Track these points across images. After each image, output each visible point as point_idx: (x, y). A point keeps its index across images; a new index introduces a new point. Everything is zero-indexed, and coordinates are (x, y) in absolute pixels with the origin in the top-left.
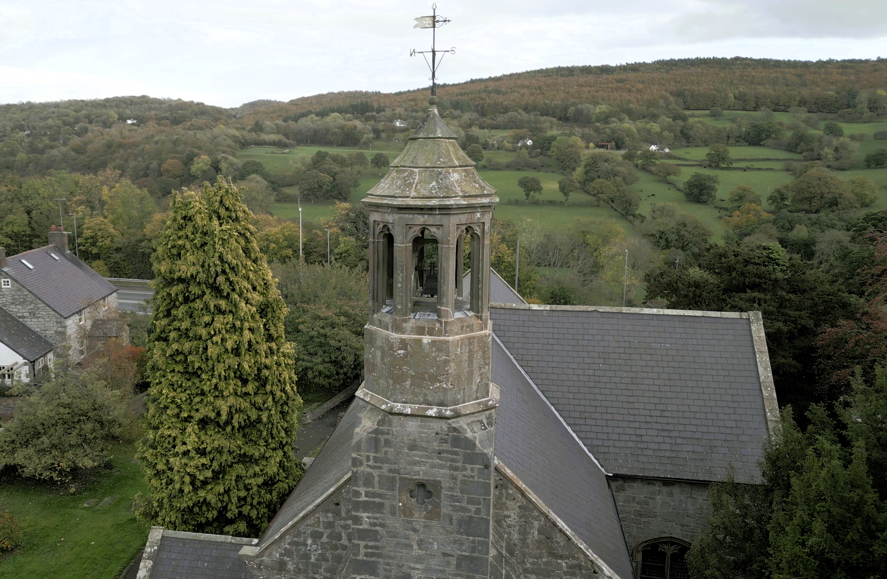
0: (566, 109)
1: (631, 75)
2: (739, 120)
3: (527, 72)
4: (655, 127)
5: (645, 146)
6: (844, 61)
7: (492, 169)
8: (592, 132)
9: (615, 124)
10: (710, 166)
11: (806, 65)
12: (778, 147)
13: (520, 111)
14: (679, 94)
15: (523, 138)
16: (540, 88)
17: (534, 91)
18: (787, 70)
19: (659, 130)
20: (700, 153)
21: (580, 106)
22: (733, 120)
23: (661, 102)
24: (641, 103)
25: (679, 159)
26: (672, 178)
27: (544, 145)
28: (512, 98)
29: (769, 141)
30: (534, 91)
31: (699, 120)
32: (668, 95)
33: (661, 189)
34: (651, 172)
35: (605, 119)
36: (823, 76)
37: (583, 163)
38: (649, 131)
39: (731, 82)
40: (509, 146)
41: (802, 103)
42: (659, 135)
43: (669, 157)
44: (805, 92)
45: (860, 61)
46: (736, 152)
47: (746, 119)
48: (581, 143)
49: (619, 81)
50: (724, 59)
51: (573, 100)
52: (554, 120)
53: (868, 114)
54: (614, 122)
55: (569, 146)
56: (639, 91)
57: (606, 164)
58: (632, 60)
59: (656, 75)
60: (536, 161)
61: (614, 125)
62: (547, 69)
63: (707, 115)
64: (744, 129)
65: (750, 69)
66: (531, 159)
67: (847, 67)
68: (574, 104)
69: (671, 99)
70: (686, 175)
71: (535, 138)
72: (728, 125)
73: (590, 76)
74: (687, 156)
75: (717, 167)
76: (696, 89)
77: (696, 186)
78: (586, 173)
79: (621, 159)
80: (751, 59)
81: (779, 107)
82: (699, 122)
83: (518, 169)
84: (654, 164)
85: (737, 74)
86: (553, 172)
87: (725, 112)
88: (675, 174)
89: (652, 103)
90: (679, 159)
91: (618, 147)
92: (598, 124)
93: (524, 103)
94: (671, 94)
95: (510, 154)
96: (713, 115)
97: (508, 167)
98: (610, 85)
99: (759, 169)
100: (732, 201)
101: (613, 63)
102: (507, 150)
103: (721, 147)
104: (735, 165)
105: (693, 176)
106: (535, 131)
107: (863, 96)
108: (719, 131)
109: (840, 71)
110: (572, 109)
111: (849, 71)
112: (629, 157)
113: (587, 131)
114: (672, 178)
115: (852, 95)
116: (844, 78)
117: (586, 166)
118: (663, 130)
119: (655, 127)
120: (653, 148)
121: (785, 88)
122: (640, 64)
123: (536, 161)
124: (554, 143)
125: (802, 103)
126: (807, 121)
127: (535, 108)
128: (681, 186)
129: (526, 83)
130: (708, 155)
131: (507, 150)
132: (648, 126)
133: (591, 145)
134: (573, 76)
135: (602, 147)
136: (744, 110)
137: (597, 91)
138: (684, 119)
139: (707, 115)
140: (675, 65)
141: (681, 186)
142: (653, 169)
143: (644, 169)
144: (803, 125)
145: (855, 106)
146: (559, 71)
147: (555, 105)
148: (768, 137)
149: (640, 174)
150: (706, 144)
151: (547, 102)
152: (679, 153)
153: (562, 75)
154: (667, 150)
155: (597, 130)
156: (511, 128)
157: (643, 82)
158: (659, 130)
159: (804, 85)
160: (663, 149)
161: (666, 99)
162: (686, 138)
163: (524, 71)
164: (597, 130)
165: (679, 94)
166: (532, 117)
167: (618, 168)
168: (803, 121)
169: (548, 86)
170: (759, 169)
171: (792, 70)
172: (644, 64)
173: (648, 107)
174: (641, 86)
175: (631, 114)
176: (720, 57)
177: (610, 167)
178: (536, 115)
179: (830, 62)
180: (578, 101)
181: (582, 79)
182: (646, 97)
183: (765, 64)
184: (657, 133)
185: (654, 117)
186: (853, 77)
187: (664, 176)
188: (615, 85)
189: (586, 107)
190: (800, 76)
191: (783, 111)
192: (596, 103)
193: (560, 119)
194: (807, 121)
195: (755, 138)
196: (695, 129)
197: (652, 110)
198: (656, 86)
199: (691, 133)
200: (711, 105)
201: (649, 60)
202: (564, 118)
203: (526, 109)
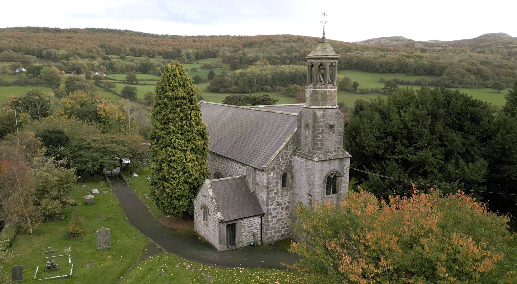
0: (41, 51)
1: (74, 34)
2: (135, 60)
3: (8, 28)
4: (96, 63)
5: (93, 73)
6: (173, 36)
7: (3, 85)
8: (62, 65)
9: (73, 61)
10: (128, 83)
11: (157, 36)
12: (155, 74)
13: (11, 51)
14: (103, 46)
15: (18, 67)
16: (20, 38)
17: (16, 40)
18: (150, 38)
19: (98, 64)
20: (123, 77)
21: (49, 50)
22: (132, 61)
23: (94, 50)
24: (84, 50)
25: (112, 79)
26: (112, 89)
27: (35, 72)
28: (3, 43)
29: (151, 72)
30: (16, 40)
31: (115, 59)
32: (97, 47)
33: (108, 95)
34: (101, 86)
35: (67, 58)
36: (166, 42)
37: (65, 82)
38: (93, 65)
39: (127, 42)
40: (11, 71)
41: (160, 54)
42: (99, 67)
43: (106, 78)
44: (160, 49)
45: (179, 36)
46: (139, 76)
47: (138, 61)
48: (58, 71)
49: (68, 37)
50: (120, 30)
51: (44, 46)
52: (35, 57)
53: (186, 60)
54: (72, 60)
55: (52, 72)
56: (81, 44)
57: (78, 82)
58: (73, 27)
59: (88, 36)
60: (33, 80)
61: (73, 61)
62: (21, 28)
63: (118, 58)
64: (138, 65)
65: (133, 36)
66: (29, 80)
67: (174, 39)
68: (44, 49)
69: (99, 49)
70: (120, 88)
71: (27, 67)
72: (131, 63)
73: (50, 33)
74: (115, 78)
75: (132, 84)
76: (110, 44)
77: (126, 93)
78: (67, 87)
79: (85, 79)
80: (133, 31)
81: (151, 55)
82: (118, 61)
83: (22, 85)
84: (102, 82)
85: (128, 38)
86: (45, 87)
87: (127, 57)
88: (114, 87)
89: (90, 51)
90: (112, 79)
91: (78, 72)
92: (63, 60)
93: (12, 46)
94: (98, 46)
95: (13, 76)
96: (122, 58)
97: (15, 84)
98: (63, 39)
99: (150, 84)
100: (145, 99)
101: (62, 27)
102: (10, 74)
103: (132, 73)
104: (140, 82)
105: (124, 88)
106: (25, 64)
107: (184, 52)
108: (127, 66)
109: (172, 40)
110: (44, 52)
111: (175, 40)
112: (88, 78)
113: (58, 64)
114: (112, 89)
115: (179, 51)
116: (174, 43)
117: (66, 83)
118: (100, 64)
119: (96, 63)
120: (97, 73)
121: (151, 47)
122: (77, 29)
123: (33, 80)
124: (41, 70)
125: (160, 54)
126: (164, 63)
127: (20, 50)
128: (120, 93)
129: (10, 35)
130: (126, 77)
131: (10, 74)
132: (92, 62)
133: (63, 72)
134: (39, 32)
135: (69, 73)
136: (135, 56)
137: (57, 42)
138: (109, 59)
139: (118, 58)
140: (97, 31)
141: (120, 93)
142: (102, 85)
143: (96, 84)
144: (162, 64)
145: (181, 56)
146: (29, 29)
147: (33, 49)
148: (150, 69)
149: (96, 87)
150: (122, 72)
151: (27, 46)
152: (111, 76)
153: (32, 32)
154: (104, 75)
155: (64, 64)
156: (7, 61)
157: (82, 39)
158: (98, 64)
159: (159, 46)
160: (102, 75)
161: (96, 49)
162: (111, 68)
163: (6, 27)
164: (64, 64)
165: (103, 46)
166: (20, 55)
167: (85, 84)
168: (162, 62)
169: (25, 37)
170: (150, 84)
171: (153, 39)
172: (79, 29)
173: (88, 53)
174: (81, 41)
175: (80, 55)
176: (118, 29)
177: (80, 84)
178: (22, 54)
179: (167, 36)
180: (47, 47)
181: (46, 35)
182: (85, 47)
183: (139, 34)
184: (97, 66)
185: (93, 58)
186: (178, 43)
187: (108, 88)
188: (66, 40)
189: (53, 51)
190: (156, 41)
191: (152, 57)
192: (59, 49)
193: (38, 57)
194: (164, 63)
195: (145, 69)
196: (116, 65)
197: (91, 54)
198: (89, 42)
199: (115, 67)
200: (119, 52)
201: (82, 27)
202: (40, 56)
203: (14, 50)
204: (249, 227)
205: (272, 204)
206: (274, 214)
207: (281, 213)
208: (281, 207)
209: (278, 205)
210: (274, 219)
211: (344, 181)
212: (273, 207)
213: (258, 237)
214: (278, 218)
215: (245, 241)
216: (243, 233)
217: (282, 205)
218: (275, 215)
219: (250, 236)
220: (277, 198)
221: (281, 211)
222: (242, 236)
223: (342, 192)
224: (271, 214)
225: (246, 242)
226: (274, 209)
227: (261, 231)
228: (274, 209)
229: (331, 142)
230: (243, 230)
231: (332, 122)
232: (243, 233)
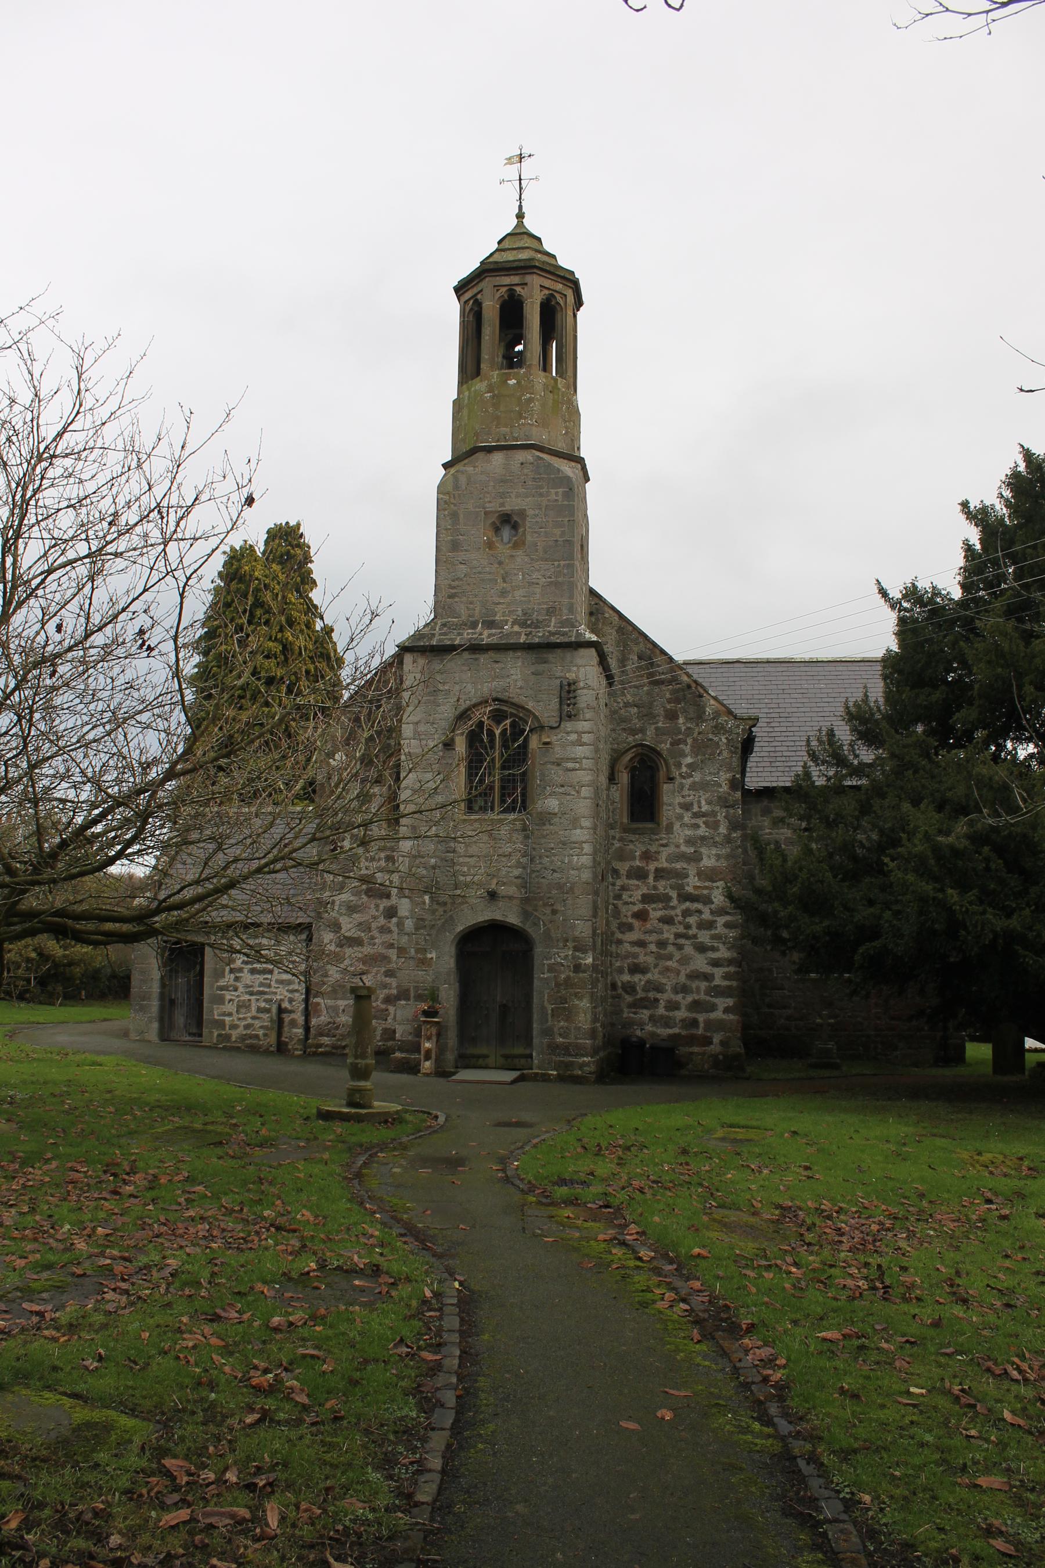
204: (253, 971)
205: (342, 887)
206: (348, 926)
207: (383, 930)
208: (384, 903)
209: (369, 893)
210: (348, 951)
211: (558, 752)
212: (345, 897)
213: (293, 1023)
214: (367, 950)
215: (234, 1027)
216: (225, 988)
217: (388, 896)
218: (354, 933)
219: (260, 1010)
220: (363, 863)
221: (382, 921)
222: (221, 1000)
223: (552, 804)
224: (336, 927)
225: (241, 1030)
226: (352, 909)
227: (307, 1000)
228: (352, 909)
229: (501, 584)
230: (229, 979)
231: (512, 504)
232: (225, 988)
